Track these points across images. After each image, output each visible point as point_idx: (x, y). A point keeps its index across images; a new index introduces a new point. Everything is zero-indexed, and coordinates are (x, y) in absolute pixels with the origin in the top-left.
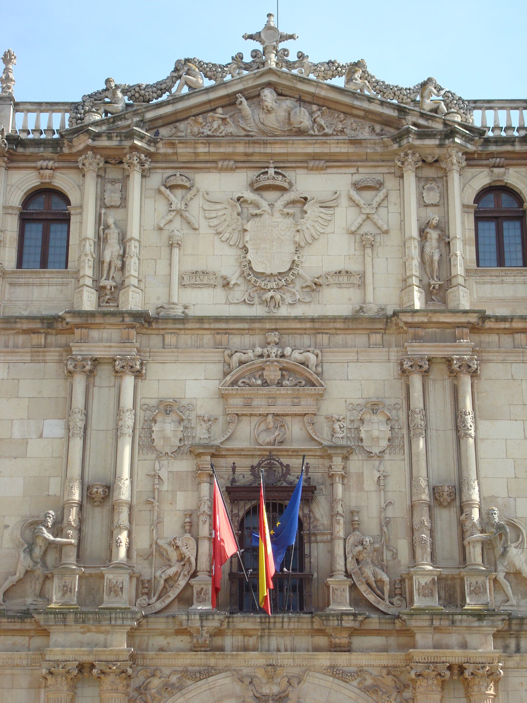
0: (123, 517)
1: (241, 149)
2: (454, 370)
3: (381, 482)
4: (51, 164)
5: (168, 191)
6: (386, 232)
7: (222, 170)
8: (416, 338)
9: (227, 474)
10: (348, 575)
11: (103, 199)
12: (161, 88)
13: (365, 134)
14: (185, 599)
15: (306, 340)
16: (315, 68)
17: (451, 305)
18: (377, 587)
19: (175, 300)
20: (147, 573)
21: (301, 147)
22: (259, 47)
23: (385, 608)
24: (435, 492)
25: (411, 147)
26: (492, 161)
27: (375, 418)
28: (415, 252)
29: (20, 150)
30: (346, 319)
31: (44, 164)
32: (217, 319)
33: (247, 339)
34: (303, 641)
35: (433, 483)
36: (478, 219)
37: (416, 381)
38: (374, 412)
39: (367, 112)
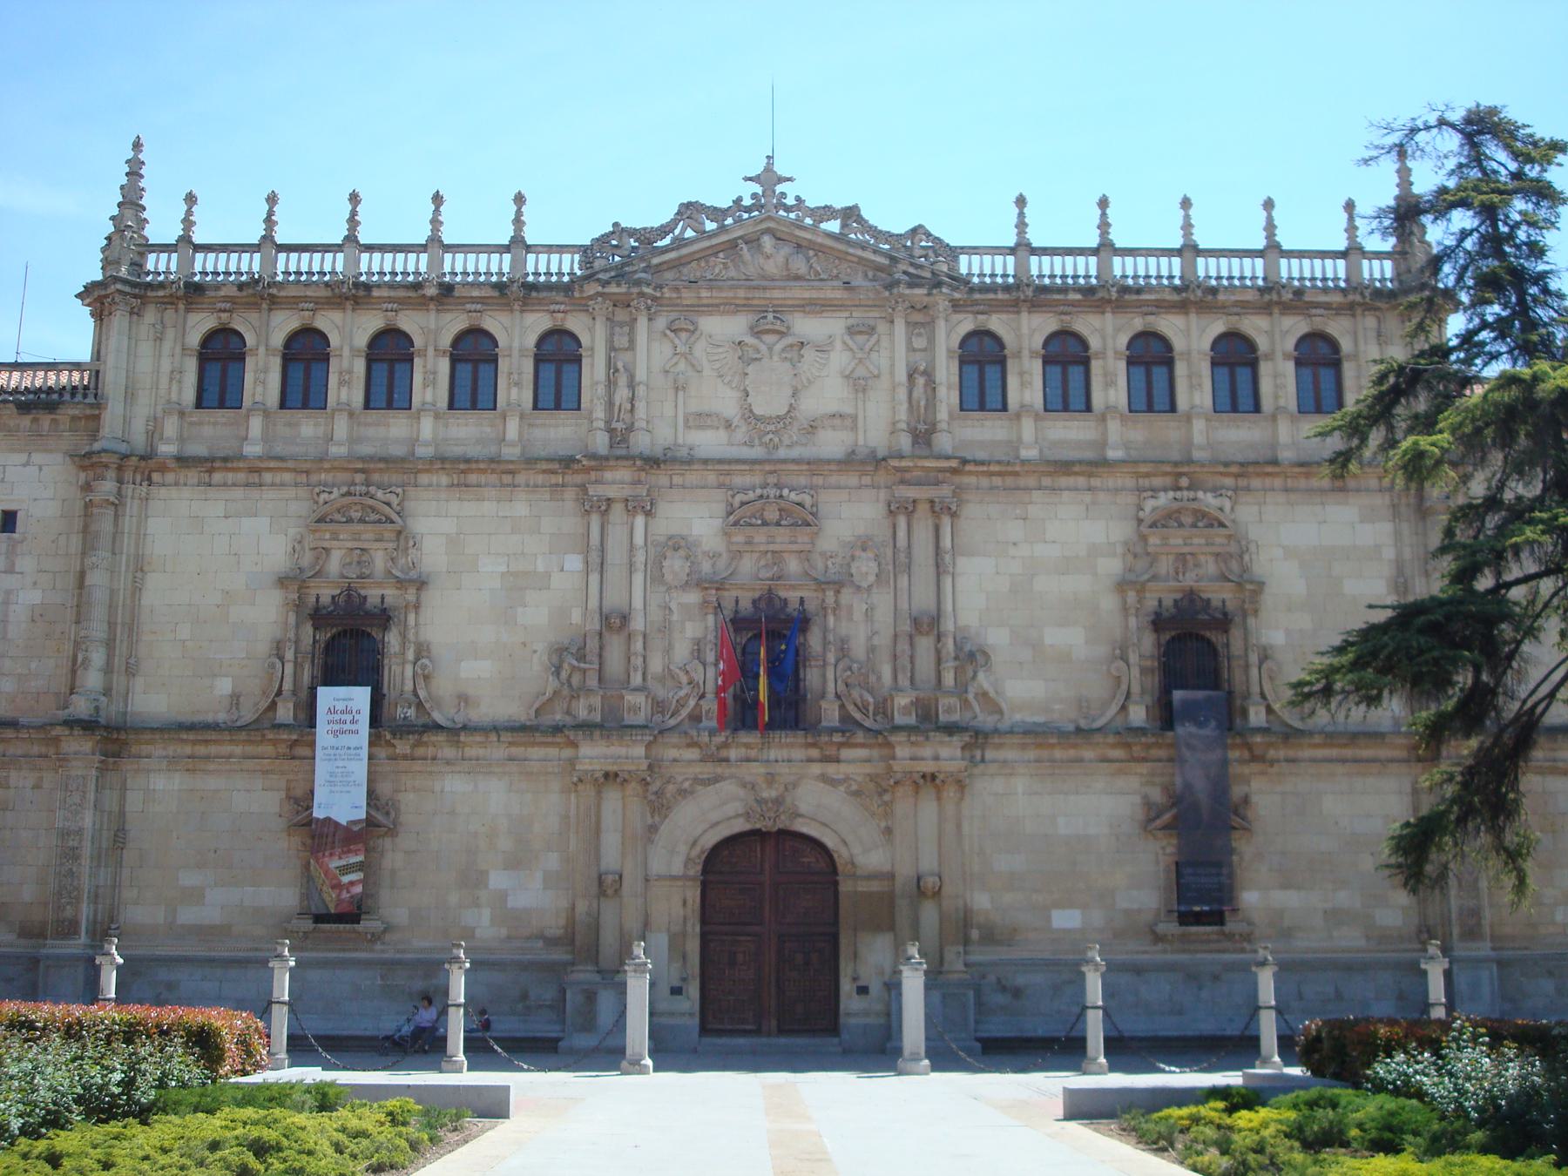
0: (638, 645)
1: (741, 293)
2: (938, 510)
4: (562, 307)
5: (672, 335)
6: (878, 377)
7: (723, 313)
8: (902, 482)
9: (728, 606)
10: (838, 696)
11: (612, 341)
12: (664, 230)
14: (695, 718)
16: (813, 212)
17: (936, 449)
18: (863, 709)
19: (680, 441)
20: (661, 693)
21: (799, 293)
22: (758, 189)
23: (870, 725)
24: (916, 622)
25: (900, 295)
26: (976, 308)
27: (864, 555)
28: (902, 394)
29: (534, 294)
30: (839, 462)
31: (557, 307)
32: (720, 461)
34: (798, 754)
35: (914, 613)
36: (962, 362)
37: (902, 521)
39: (860, 258)
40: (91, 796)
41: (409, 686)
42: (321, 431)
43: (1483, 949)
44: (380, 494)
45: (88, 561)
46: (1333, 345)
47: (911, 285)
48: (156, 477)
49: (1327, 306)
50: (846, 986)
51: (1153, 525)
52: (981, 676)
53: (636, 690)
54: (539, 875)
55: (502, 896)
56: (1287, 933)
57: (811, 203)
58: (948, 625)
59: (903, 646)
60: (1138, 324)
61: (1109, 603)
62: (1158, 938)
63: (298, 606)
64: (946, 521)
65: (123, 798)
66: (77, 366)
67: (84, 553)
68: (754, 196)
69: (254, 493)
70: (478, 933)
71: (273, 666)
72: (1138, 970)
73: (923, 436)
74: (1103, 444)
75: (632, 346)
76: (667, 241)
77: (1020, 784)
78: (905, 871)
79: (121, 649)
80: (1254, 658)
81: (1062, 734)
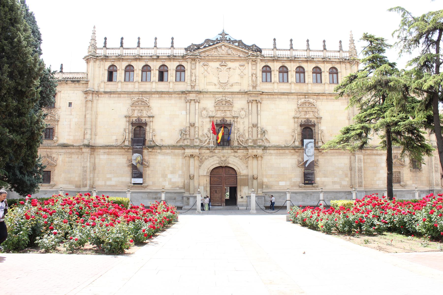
0: (197, 129)
8: (250, 96)
12: (202, 45)
13: (241, 55)
15: (230, 96)
22: (221, 36)
24: (253, 125)
28: (251, 79)
30: (238, 92)
32: (214, 92)
33: (219, 96)
36: (263, 72)
37: (250, 104)
38: (243, 110)
40: (89, 159)
41: (151, 137)
43: (362, 189)
44: (145, 99)
45: (87, 112)
47: (252, 56)
49: (335, 62)
50: (239, 197)
51: (301, 105)
52: (266, 136)
53: (196, 138)
55: (171, 179)
56: (325, 186)
57: (232, 39)
58: (259, 125)
59: (250, 129)
60: (298, 65)
61: (292, 121)
62: (300, 187)
64: (259, 104)
65: (95, 160)
67: (86, 111)
68: (220, 38)
69: (120, 99)
71: (124, 133)
72: (296, 193)
73: (254, 87)
74: (291, 89)
75: (195, 68)
76: (203, 47)
77: (273, 157)
78: (250, 174)
79: (94, 130)
80: (320, 132)
81: (282, 147)
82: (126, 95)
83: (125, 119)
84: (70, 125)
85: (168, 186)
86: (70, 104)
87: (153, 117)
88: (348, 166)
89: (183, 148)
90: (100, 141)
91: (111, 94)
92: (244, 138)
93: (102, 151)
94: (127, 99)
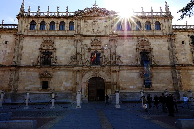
3: (107, 52)
8: (111, 37)
12: (84, 11)
14: (87, 64)
15: (100, 38)
18: (107, 63)
30: (104, 36)
37: (111, 42)
40: (14, 74)
41: (54, 61)
42: (44, 32)
46: (159, 22)
48: (24, 37)
52: (120, 59)
53: (81, 61)
54: (69, 82)
55: (65, 85)
56: (158, 89)
58: (117, 53)
59: (111, 56)
61: (135, 51)
63: (41, 52)
64: (116, 42)
66: (15, 25)
70: (62, 90)
75: (80, 23)
77: (125, 72)
79: (19, 57)
80: (152, 57)
82: (40, 37)
83: (39, 51)
84: (5, 54)
85: (63, 89)
86: (6, 42)
87: (56, 49)
88: (172, 76)
89: (72, 66)
90: (23, 63)
91: (31, 36)
92: (108, 61)
93: (23, 69)
94: (41, 39)
